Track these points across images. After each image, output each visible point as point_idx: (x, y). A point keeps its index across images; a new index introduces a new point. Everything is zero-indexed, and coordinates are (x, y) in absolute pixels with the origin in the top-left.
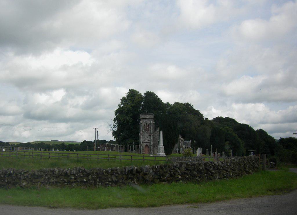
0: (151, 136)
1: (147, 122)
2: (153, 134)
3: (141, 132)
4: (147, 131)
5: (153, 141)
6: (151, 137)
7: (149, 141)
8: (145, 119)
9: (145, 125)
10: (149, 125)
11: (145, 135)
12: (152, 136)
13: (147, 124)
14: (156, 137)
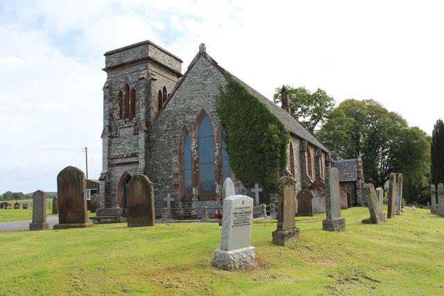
1: (127, 79)
2: (147, 126)
4: (126, 116)
5: (147, 158)
7: (134, 159)
9: (121, 93)
10: (134, 91)
11: (122, 132)
12: (142, 135)
13: (127, 87)
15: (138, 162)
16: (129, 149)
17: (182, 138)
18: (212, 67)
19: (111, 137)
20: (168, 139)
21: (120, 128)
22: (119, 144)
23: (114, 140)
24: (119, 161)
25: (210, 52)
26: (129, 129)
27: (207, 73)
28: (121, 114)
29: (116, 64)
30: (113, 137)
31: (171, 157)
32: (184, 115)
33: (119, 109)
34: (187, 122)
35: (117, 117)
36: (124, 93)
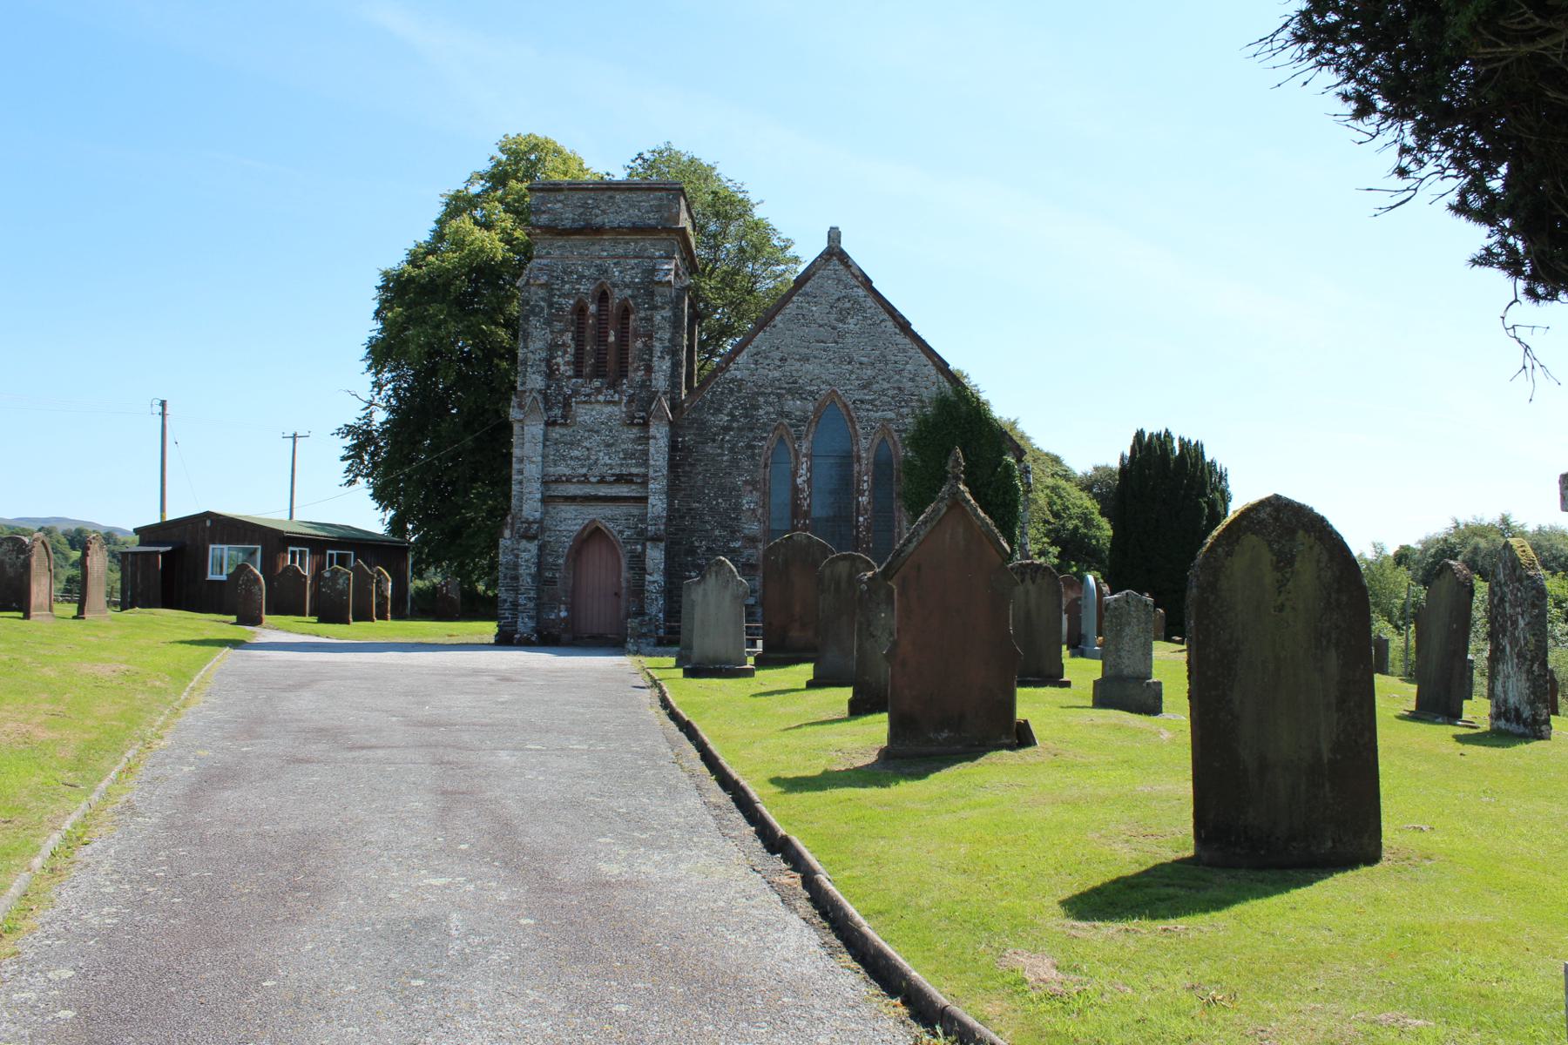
0: (645, 425)
1: (603, 271)
3: (534, 381)
4: (597, 372)
5: (672, 491)
6: (645, 439)
7: (623, 490)
8: (591, 231)
9: (580, 310)
10: (625, 312)
11: (584, 414)
12: (660, 434)
13: (603, 297)
14: (710, 448)
15: (644, 499)
16: (608, 462)
17: (770, 452)
18: (861, 292)
19: (550, 423)
20: (731, 450)
21: (577, 403)
22: (572, 444)
23: (556, 433)
24: (573, 490)
25: (845, 245)
26: (607, 410)
27: (848, 305)
28: (578, 363)
29: (568, 224)
30: (554, 423)
31: (739, 497)
32: (779, 396)
33: (571, 350)
34: (788, 415)
35: (565, 369)
36: (592, 308)
